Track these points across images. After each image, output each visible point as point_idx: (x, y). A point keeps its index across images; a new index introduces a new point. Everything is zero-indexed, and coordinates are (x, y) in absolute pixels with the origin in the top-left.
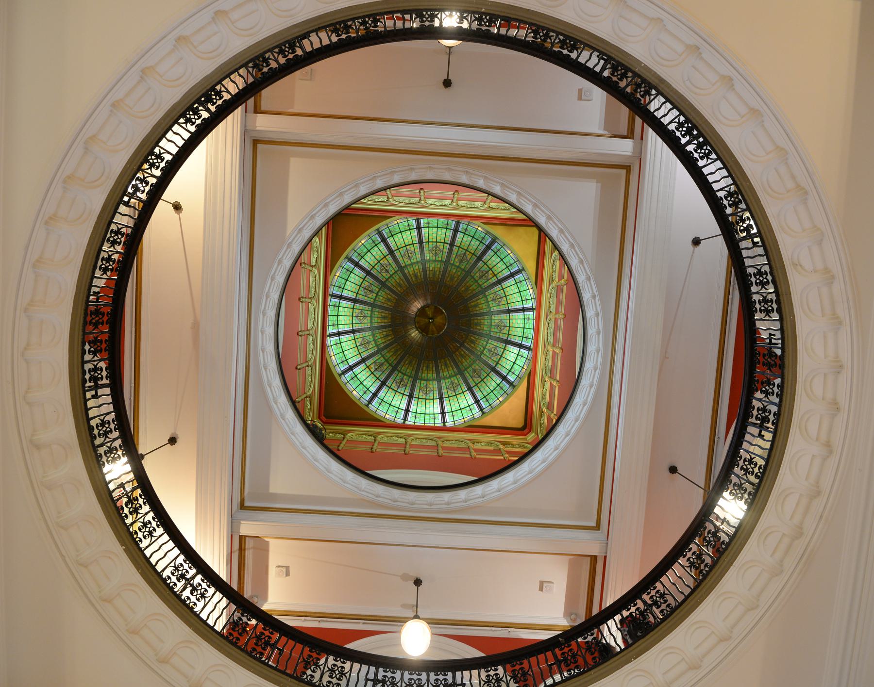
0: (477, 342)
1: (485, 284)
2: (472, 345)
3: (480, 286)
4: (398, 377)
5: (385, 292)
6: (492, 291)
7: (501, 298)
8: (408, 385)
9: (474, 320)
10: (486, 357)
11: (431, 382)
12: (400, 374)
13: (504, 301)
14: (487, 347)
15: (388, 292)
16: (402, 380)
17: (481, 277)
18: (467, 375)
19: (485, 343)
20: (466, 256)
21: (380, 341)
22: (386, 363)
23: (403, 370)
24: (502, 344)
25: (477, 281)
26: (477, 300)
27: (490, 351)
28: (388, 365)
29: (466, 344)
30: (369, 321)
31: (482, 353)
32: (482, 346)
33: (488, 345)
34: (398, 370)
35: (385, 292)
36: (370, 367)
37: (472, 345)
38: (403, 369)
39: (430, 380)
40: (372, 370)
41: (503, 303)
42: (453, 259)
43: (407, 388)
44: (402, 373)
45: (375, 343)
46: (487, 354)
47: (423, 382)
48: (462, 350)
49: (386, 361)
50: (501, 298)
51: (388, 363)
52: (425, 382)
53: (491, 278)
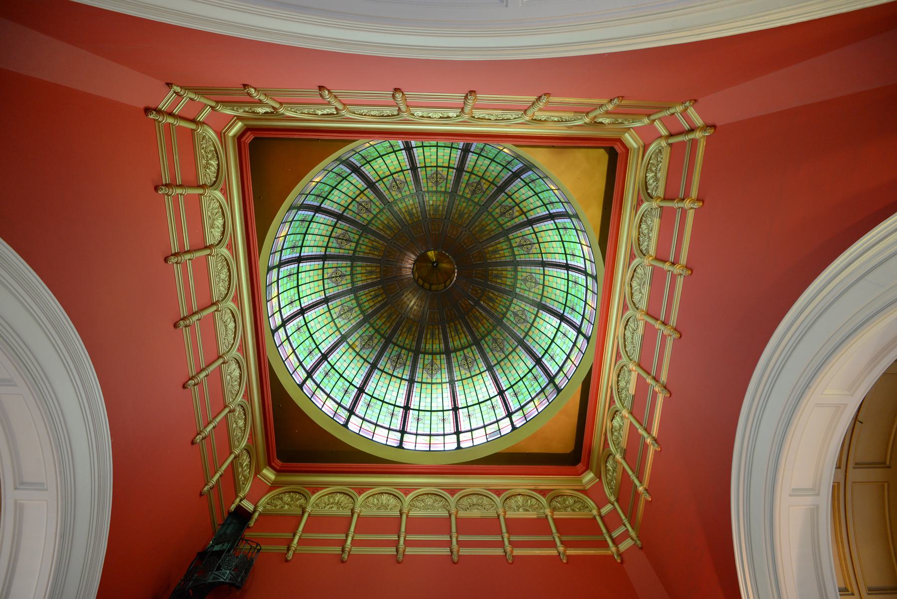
0: (497, 301)
1: (509, 224)
2: (491, 304)
3: (501, 225)
4: (394, 353)
5: (369, 239)
6: (518, 233)
7: (532, 244)
8: (408, 363)
9: (492, 270)
10: (510, 322)
11: (438, 357)
12: (396, 348)
13: (535, 249)
14: (512, 308)
15: (373, 238)
16: (399, 357)
17: (503, 214)
18: (486, 346)
19: (508, 303)
20: (480, 184)
21: (367, 305)
22: (376, 335)
23: (401, 342)
24: (533, 307)
25: (496, 220)
26: (497, 244)
27: (515, 315)
28: (379, 337)
29: (482, 303)
30: (349, 281)
31: (504, 315)
32: (504, 306)
33: (513, 305)
34: (393, 343)
35: (369, 239)
36: (353, 346)
37: (491, 304)
38: (400, 339)
39: (436, 354)
40: (357, 350)
41: (534, 251)
42: (462, 189)
43: (407, 367)
44: (399, 346)
45: (360, 309)
46: (512, 319)
47: (427, 356)
48: (478, 310)
49: (377, 331)
50: (532, 244)
51: (379, 334)
52: (430, 357)
53: (517, 217)
